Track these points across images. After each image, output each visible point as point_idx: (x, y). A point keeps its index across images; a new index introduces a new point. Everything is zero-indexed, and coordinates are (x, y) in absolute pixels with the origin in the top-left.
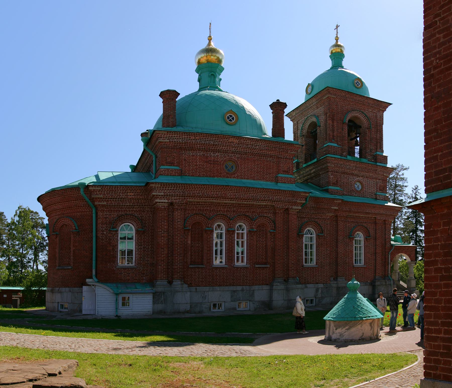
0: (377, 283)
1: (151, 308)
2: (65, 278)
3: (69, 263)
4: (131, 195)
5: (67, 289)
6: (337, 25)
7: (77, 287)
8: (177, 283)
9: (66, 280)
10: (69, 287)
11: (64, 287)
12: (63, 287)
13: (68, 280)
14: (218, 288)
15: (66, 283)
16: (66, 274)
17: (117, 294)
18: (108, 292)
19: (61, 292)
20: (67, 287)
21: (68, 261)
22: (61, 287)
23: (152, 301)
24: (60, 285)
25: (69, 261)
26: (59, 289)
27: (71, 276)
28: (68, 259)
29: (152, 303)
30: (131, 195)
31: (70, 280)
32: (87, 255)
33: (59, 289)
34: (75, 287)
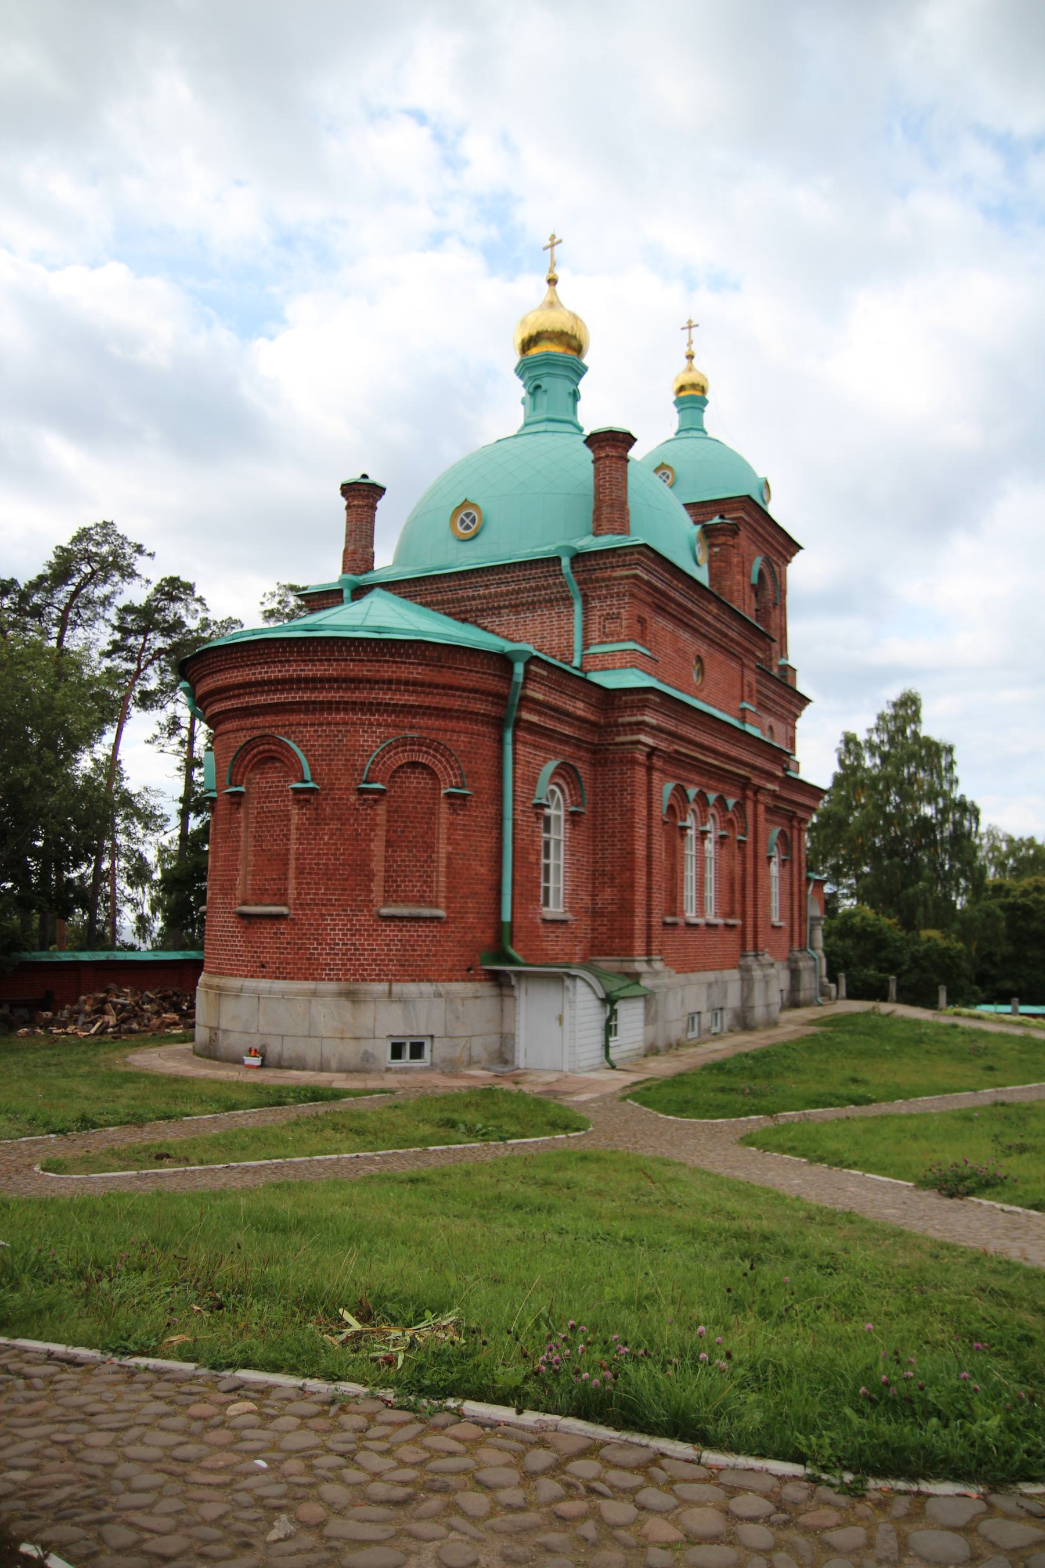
0: (801, 964)
1: (641, 1038)
2: (416, 950)
3: (422, 896)
4: (579, 708)
5: (426, 988)
6: (690, 322)
7: (457, 980)
8: (658, 965)
9: (419, 955)
10: (429, 981)
11: (413, 981)
12: (407, 981)
13: (427, 955)
14: (692, 976)
15: (419, 966)
16: (419, 936)
17: (609, 1001)
18: (592, 997)
19: (402, 1000)
20: (421, 981)
21: (418, 891)
22: (398, 981)
23: (642, 1017)
24: (393, 975)
25: (425, 891)
26: (390, 992)
27: (439, 941)
28: (418, 881)
29: (642, 1024)
30: (579, 708)
31: (434, 955)
32: (482, 874)
33: (390, 992)
34: (450, 980)
